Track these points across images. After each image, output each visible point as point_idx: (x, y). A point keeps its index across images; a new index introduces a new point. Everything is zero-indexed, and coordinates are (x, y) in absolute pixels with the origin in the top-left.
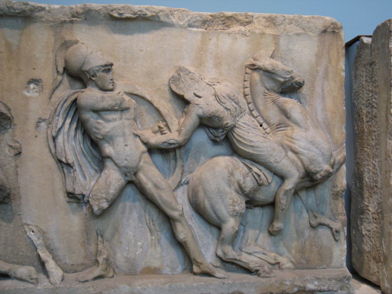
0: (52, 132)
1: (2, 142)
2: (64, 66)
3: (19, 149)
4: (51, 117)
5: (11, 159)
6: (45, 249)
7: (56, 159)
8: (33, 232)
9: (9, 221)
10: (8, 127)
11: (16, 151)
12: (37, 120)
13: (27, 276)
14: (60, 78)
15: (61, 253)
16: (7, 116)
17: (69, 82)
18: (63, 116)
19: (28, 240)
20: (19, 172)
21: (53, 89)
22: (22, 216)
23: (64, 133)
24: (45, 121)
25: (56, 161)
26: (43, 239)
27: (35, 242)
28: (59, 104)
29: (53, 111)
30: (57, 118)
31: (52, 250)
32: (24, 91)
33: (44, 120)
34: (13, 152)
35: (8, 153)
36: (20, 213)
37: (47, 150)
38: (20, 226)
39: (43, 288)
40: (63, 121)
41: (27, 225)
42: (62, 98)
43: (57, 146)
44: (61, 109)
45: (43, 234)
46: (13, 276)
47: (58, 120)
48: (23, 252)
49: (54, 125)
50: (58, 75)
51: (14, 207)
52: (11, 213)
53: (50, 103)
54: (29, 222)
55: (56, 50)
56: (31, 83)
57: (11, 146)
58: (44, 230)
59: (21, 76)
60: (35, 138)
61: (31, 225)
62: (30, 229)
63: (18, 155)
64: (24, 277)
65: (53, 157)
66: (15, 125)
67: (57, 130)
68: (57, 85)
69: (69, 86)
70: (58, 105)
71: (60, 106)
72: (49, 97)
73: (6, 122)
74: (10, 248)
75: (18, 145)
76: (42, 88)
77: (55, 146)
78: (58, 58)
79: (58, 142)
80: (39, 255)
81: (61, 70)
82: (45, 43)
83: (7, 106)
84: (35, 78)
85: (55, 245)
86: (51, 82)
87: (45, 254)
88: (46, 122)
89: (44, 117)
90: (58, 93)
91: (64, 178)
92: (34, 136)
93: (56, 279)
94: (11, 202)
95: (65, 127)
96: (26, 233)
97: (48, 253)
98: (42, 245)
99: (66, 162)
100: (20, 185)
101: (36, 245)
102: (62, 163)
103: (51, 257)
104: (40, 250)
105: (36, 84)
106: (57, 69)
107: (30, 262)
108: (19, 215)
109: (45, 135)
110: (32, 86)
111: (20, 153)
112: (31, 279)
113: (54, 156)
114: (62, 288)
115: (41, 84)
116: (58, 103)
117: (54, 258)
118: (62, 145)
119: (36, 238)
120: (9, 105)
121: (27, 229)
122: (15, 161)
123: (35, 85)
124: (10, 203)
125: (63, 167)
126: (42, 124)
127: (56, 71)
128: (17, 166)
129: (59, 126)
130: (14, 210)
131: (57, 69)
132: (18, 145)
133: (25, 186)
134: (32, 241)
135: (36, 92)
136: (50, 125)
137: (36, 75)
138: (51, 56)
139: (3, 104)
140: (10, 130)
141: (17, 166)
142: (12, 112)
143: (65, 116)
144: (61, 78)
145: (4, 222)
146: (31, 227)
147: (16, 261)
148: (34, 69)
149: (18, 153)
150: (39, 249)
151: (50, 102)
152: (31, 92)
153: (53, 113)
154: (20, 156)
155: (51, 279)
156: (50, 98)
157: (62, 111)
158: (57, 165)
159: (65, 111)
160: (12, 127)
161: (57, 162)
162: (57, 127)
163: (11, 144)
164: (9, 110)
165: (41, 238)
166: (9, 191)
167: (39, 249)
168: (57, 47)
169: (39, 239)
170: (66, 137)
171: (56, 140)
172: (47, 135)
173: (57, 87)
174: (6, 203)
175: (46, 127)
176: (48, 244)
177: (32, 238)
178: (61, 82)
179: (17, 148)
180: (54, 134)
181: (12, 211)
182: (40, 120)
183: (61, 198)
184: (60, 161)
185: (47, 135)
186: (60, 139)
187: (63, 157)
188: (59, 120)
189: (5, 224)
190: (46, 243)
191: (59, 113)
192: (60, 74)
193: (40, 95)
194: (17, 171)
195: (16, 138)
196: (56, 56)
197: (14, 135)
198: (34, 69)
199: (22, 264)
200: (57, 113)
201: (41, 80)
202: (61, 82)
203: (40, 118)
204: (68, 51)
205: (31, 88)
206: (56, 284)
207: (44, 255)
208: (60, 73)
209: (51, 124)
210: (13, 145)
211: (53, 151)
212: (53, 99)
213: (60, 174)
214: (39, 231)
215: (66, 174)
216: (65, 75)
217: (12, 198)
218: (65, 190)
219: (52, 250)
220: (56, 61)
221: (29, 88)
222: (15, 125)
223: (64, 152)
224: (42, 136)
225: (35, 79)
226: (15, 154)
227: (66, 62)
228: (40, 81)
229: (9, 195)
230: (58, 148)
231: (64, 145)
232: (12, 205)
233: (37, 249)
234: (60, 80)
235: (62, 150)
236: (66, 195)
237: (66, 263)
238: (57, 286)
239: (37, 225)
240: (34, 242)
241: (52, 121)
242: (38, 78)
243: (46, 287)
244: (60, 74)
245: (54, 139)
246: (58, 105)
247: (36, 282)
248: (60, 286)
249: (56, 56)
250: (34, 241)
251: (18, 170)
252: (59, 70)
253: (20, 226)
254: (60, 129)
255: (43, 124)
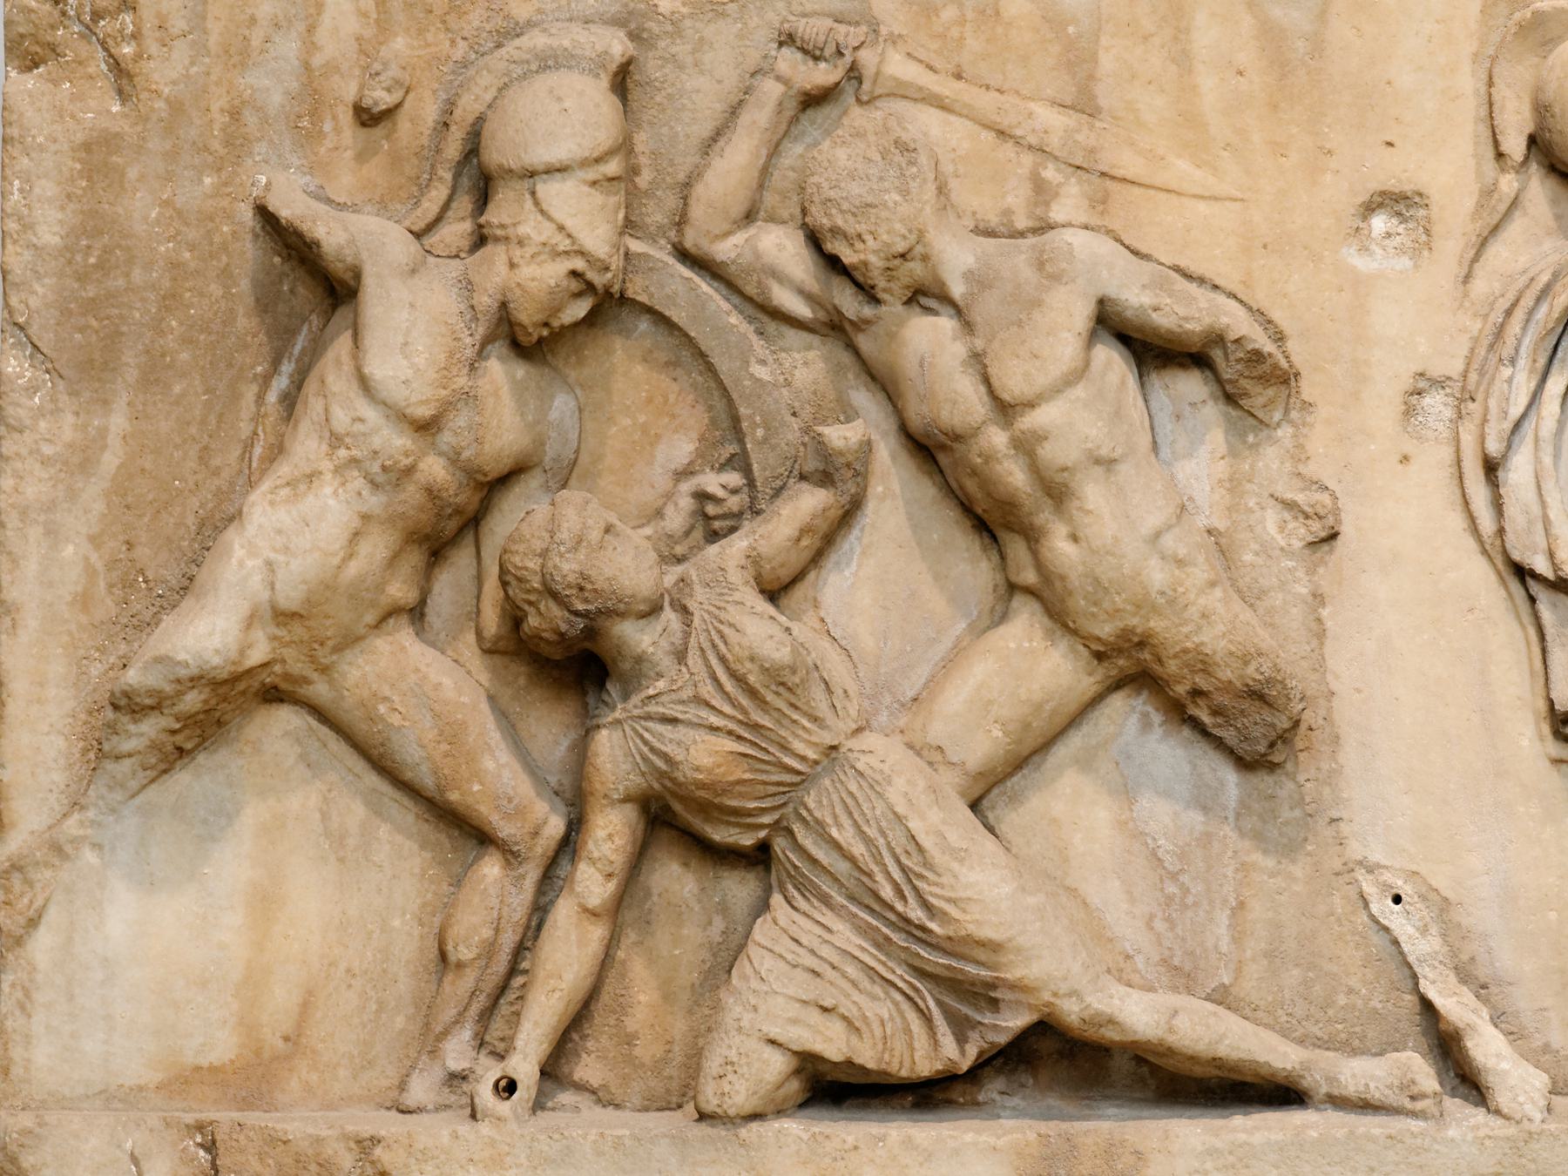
0: (1482, 439)
1: (1248, 486)
2: (1529, 128)
3: (1330, 521)
4: (1476, 367)
5: (1290, 564)
6: (1453, 978)
7: (1499, 561)
8: (1397, 899)
9: (1289, 849)
10: (1277, 416)
11: (1316, 526)
12: (1407, 383)
13: (1390, 1087)
14: (1508, 183)
15: (1522, 1001)
16: (1276, 366)
17: (1554, 202)
18: (1535, 361)
19: (1377, 939)
20: (1329, 624)
21: (1478, 236)
22: (1344, 828)
23: (1537, 440)
24: (1443, 388)
25: (1499, 573)
26: (1444, 935)
27: (1406, 947)
28: (1515, 304)
29: (1486, 342)
30: (1506, 372)
31: (1484, 987)
32: (1344, 250)
33: (1439, 383)
34: (1301, 532)
35: (1279, 537)
36: (1336, 815)
37: (1457, 521)
38: (1337, 874)
39: (1470, 1137)
40: (1533, 385)
41: (1370, 871)
42: (1523, 280)
43: (1506, 500)
44: (1524, 329)
45: (1442, 910)
46: (1324, 1090)
47: (1510, 381)
48: (1350, 991)
49: (1492, 403)
50: (1503, 170)
51: (1308, 785)
52: (1297, 813)
53: (1467, 304)
54: (1376, 856)
55: (1491, 52)
56: (1377, 212)
57: (1290, 505)
58: (1446, 893)
59: (1328, 177)
60: (1400, 467)
61: (1386, 867)
62: (1386, 886)
63: (1326, 547)
64: (1376, 1094)
65: (1485, 552)
66: (1307, 406)
67: (1508, 425)
68: (1497, 217)
69: (1552, 223)
70: (1509, 313)
71: (1519, 315)
72: (1463, 274)
73: (1271, 392)
74: (1295, 972)
75: (1325, 498)
76: (1427, 232)
77: (1498, 505)
78: (1501, 92)
79: (1510, 481)
80: (1427, 1006)
81: (1515, 145)
82: (1437, 22)
83: (1270, 322)
84: (1392, 185)
85: (1497, 964)
86: (1469, 203)
87: (1455, 999)
88: (1448, 390)
89: (1437, 370)
90: (1500, 254)
91: (1536, 650)
92: (1399, 457)
93: (1521, 1099)
94: (1297, 764)
95: (1544, 413)
96: (1366, 905)
97: (1468, 996)
98: (1441, 962)
99: (1550, 575)
100: (1334, 686)
101: (1411, 959)
102: (1530, 582)
103: (1485, 1013)
104: (1433, 982)
105: (1399, 214)
106: (1496, 143)
107: (1385, 1039)
108: (1333, 820)
109: (1446, 453)
110: (1380, 223)
111: (1333, 536)
112: (1413, 1098)
113: (1488, 547)
114: (1556, 1138)
115: (1422, 212)
116: (1504, 304)
117: (1498, 1019)
118: (1530, 495)
119: (1411, 930)
120: (1277, 315)
121: (1369, 889)
122: (1311, 572)
123: (1395, 221)
124: (1289, 766)
125: (1532, 600)
126: (1427, 400)
127: (1490, 153)
128: (1318, 598)
129: (1516, 411)
130: (1308, 799)
131: (1496, 143)
132: (1325, 498)
133: (1358, 691)
134: (1396, 943)
135: (1401, 251)
136: (1471, 406)
137: (1395, 171)
138: (1468, 83)
139: (1250, 309)
140: (1285, 432)
141: (1318, 598)
142: (1291, 345)
143: (1542, 361)
144: (1516, 184)
145: (1265, 852)
146: (1387, 877)
147: (1319, 1034)
148: (1390, 144)
149: (1323, 534)
150: (1425, 977)
151: (1466, 295)
152: (1378, 251)
153: (1482, 351)
154: (1331, 551)
155: (1502, 1099)
156: (1467, 278)
157: (1527, 341)
158: (1503, 593)
159: (1542, 339)
160: (1294, 414)
161: (1505, 574)
162: (1506, 413)
163: (1289, 496)
164: (1279, 338)
165: (1434, 930)
166: (1301, 706)
167: (1425, 977)
168: (1495, 38)
169: (1424, 931)
170: (1547, 460)
171: (1500, 474)
172: (1458, 451)
173: (1495, 229)
174: (1273, 767)
175: (1449, 413)
176: (1465, 957)
177: (1392, 926)
178: (1515, 203)
179: (1322, 512)
180: (1494, 447)
181: (1300, 802)
182: (1422, 384)
183: (1525, 743)
184: (1521, 572)
185: (1458, 451)
186: (1518, 473)
187: (1535, 553)
188: (1515, 381)
189: (1270, 863)
190: (1454, 953)
191: (1517, 350)
192: (1513, 167)
193: (1416, 266)
194: (1319, 620)
195: (1309, 470)
196: (1490, 84)
197: (1299, 454)
198: (1390, 144)
199: (1352, 1048)
200: (1507, 352)
201: (1420, 195)
202: (1515, 203)
203: (1421, 375)
204: (1551, 58)
205: (1373, 235)
206: (1525, 1121)
207: (1454, 1004)
208: (1509, 162)
209: (1473, 400)
210: (1300, 498)
211: (1487, 524)
212: (1481, 286)
213: (1519, 634)
214: (1423, 898)
215: (1550, 631)
216: (1534, 167)
217: (1300, 744)
218: (1542, 705)
219: (1484, 987)
220: (1491, 105)
221: (1366, 232)
222: (1307, 406)
223: (1540, 526)
224: (1433, 461)
225: (1397, 191)
226: (1311, 539)
227: (1541, 110)
228: (1417, 199)
229: (1297, 724)
230: (1510, 510)
231: (1540, 495)
232: (1301, 778)
233: (1415, 977)
234: (1513, 195)
235: (1530, 522)
236: (1546, 729)
237: (1546, 1048)
238: (1534, 1127)
239: (1414, 868)
240: (1403, 945)
241: (1478, 384)
242: (1408, 188)
243: (1481, 1133)
244: (1513, 167)
245: (1491, 468)
246: (1509, 313)
247: (1435, 1111)
248: (1545, 1126)
249: (1490, 84)
250: (1402, 939)
251: (1325, 613)
252: (1504, 148)
253: (1337, 874)
254: (1518, 425)
255: (1436, 404)
